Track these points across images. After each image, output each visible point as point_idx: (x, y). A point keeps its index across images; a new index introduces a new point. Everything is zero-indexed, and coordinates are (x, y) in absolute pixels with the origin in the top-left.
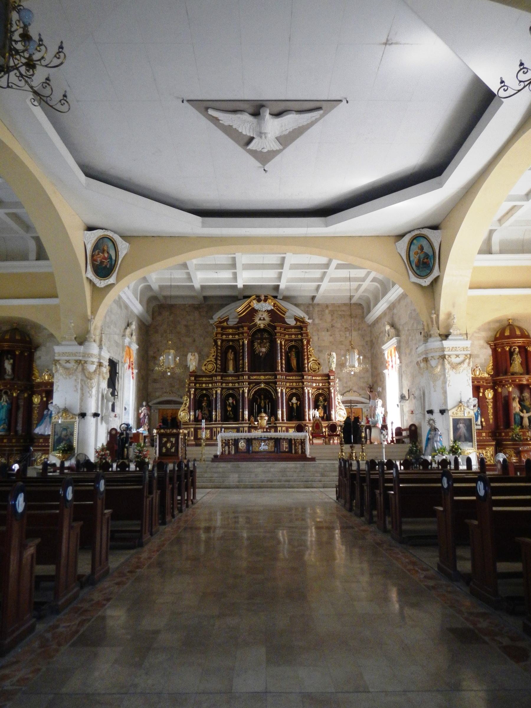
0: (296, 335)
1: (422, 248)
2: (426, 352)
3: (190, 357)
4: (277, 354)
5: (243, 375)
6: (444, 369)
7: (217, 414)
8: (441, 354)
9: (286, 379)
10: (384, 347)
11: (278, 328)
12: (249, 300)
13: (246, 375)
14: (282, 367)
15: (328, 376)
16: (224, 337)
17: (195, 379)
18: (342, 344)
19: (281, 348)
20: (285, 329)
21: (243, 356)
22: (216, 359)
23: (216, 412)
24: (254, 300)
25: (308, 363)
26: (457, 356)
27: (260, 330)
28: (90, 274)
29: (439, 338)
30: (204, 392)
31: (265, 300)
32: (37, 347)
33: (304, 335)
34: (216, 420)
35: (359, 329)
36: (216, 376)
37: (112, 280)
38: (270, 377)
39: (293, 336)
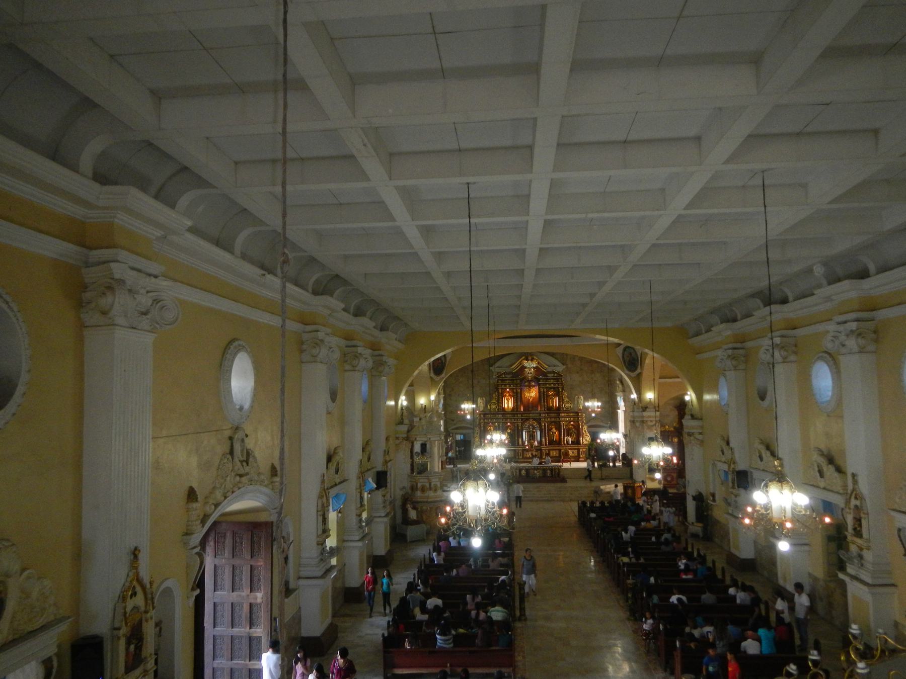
1: (631, 354)
2: (633, 417)
3: (479, 400)
5: (517, 414)
8: (642, 419)
9: (547, 416)
10: (617, 393)
11: (541, 381)
12: (520, 360)
13: (519, 414)
14: (544, 407)
15: (577, 413)
16: (503, 386)
17: (484, 417)
18: (589, 383)
19: (544, 395)
24: (524, 359)
26: (651, 421)
28: (432, 375)
29: (641, 410)
31: (532, 360)
33: (560, 385)
36: (499, 414)
37: (443, 375)
38: (536, 415)
39: (552, 385)
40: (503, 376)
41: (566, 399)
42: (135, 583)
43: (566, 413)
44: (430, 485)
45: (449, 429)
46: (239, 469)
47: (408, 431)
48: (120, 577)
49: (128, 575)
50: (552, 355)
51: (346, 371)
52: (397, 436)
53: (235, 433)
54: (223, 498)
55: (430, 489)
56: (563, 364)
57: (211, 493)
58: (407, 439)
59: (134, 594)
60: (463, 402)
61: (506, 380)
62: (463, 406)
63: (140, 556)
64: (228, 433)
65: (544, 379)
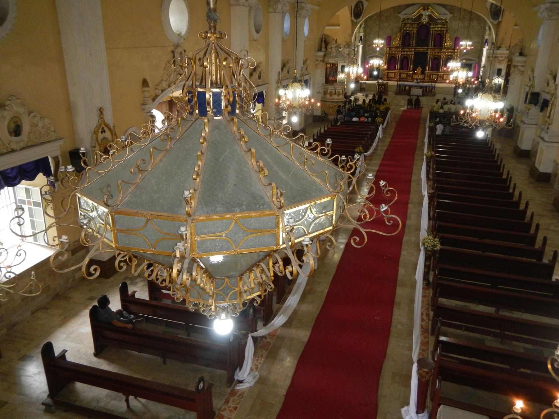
0: (440, 28)
4: (430, 39)
5: (412, 48)
6: (495, 62)
7: (398, 66)
11: (432, 25)
13: (413, 48)
14: (431, 45)
16: (405, 28)
17: (389, 49)
19: (432, 35)
20: (436, 25)
21: (413, 38)
22: (400, 39)
23: (398, 65)
25: (445, 43)
27: (423, 25)
28: (353, 19)
30: (393, 55)
31: (428, 9)
32: (329, 43)
34: (397, 70)
35: (479, 19)
36: (399, 48)
37: (360, 19)
38: (425, 50)
39: (440, 29)
40: (406, 21)
41: (448, 39)
42: (103, 126)
43: (446, 49)
44: (335, 91)
45: (366, 57)
46: (179, 71)
47: (324, 56)
48: (94, 121)
49: (99, 121)
50: (444, 6)
51: (270, 12)
52: (317, 59)
53: (176, 49)
54: (168, 87)
55: (335, 94)
56: (451, 13)
57: (159, 83)
58: (323, 61)
59: (103, 131)
60: (375, 38)
61: (408, 24)
62: (376, 41)
63: (104, 112)
64: (172, 48)
65: (434, 24)
